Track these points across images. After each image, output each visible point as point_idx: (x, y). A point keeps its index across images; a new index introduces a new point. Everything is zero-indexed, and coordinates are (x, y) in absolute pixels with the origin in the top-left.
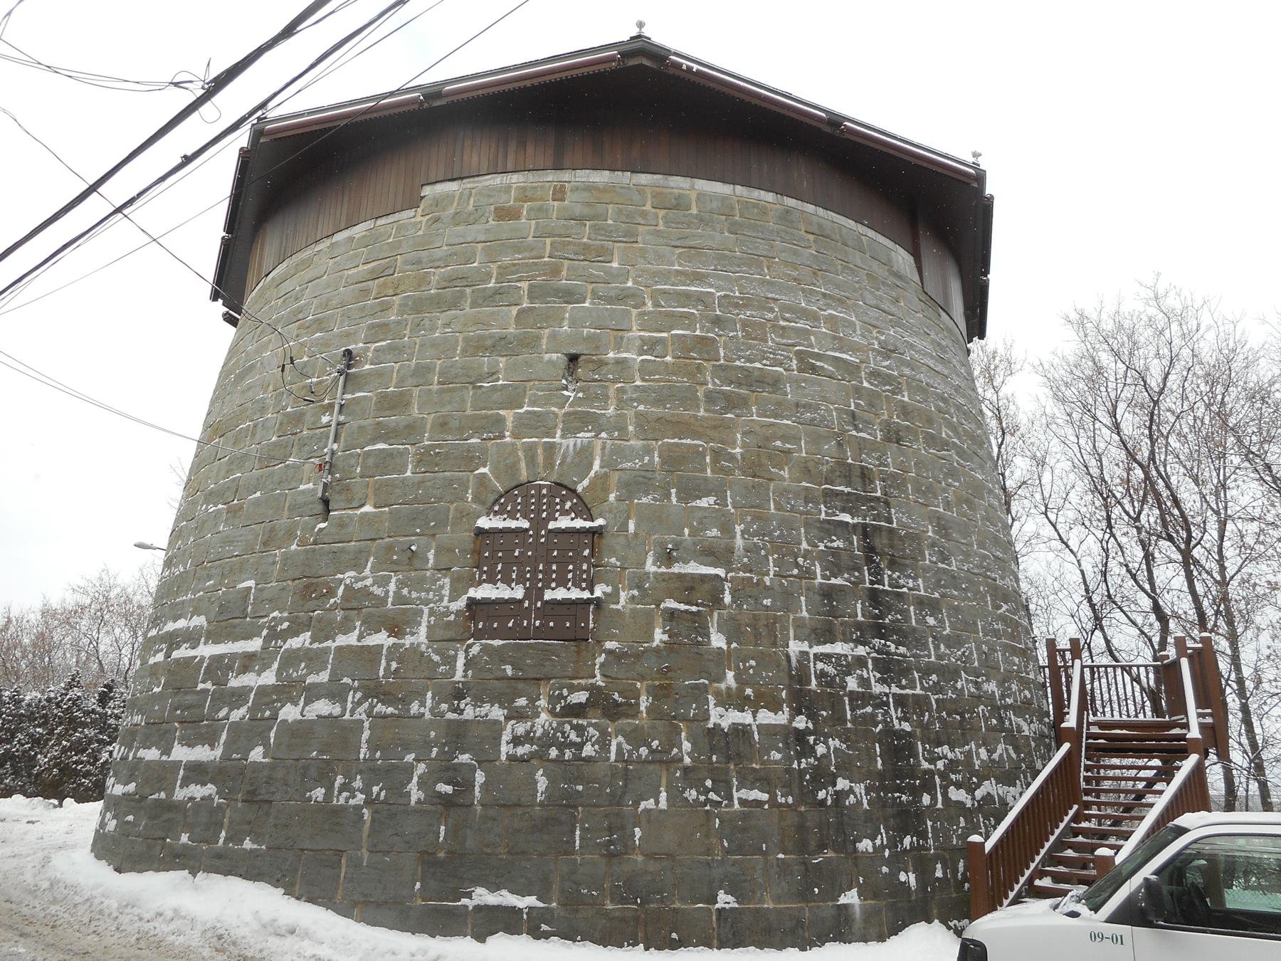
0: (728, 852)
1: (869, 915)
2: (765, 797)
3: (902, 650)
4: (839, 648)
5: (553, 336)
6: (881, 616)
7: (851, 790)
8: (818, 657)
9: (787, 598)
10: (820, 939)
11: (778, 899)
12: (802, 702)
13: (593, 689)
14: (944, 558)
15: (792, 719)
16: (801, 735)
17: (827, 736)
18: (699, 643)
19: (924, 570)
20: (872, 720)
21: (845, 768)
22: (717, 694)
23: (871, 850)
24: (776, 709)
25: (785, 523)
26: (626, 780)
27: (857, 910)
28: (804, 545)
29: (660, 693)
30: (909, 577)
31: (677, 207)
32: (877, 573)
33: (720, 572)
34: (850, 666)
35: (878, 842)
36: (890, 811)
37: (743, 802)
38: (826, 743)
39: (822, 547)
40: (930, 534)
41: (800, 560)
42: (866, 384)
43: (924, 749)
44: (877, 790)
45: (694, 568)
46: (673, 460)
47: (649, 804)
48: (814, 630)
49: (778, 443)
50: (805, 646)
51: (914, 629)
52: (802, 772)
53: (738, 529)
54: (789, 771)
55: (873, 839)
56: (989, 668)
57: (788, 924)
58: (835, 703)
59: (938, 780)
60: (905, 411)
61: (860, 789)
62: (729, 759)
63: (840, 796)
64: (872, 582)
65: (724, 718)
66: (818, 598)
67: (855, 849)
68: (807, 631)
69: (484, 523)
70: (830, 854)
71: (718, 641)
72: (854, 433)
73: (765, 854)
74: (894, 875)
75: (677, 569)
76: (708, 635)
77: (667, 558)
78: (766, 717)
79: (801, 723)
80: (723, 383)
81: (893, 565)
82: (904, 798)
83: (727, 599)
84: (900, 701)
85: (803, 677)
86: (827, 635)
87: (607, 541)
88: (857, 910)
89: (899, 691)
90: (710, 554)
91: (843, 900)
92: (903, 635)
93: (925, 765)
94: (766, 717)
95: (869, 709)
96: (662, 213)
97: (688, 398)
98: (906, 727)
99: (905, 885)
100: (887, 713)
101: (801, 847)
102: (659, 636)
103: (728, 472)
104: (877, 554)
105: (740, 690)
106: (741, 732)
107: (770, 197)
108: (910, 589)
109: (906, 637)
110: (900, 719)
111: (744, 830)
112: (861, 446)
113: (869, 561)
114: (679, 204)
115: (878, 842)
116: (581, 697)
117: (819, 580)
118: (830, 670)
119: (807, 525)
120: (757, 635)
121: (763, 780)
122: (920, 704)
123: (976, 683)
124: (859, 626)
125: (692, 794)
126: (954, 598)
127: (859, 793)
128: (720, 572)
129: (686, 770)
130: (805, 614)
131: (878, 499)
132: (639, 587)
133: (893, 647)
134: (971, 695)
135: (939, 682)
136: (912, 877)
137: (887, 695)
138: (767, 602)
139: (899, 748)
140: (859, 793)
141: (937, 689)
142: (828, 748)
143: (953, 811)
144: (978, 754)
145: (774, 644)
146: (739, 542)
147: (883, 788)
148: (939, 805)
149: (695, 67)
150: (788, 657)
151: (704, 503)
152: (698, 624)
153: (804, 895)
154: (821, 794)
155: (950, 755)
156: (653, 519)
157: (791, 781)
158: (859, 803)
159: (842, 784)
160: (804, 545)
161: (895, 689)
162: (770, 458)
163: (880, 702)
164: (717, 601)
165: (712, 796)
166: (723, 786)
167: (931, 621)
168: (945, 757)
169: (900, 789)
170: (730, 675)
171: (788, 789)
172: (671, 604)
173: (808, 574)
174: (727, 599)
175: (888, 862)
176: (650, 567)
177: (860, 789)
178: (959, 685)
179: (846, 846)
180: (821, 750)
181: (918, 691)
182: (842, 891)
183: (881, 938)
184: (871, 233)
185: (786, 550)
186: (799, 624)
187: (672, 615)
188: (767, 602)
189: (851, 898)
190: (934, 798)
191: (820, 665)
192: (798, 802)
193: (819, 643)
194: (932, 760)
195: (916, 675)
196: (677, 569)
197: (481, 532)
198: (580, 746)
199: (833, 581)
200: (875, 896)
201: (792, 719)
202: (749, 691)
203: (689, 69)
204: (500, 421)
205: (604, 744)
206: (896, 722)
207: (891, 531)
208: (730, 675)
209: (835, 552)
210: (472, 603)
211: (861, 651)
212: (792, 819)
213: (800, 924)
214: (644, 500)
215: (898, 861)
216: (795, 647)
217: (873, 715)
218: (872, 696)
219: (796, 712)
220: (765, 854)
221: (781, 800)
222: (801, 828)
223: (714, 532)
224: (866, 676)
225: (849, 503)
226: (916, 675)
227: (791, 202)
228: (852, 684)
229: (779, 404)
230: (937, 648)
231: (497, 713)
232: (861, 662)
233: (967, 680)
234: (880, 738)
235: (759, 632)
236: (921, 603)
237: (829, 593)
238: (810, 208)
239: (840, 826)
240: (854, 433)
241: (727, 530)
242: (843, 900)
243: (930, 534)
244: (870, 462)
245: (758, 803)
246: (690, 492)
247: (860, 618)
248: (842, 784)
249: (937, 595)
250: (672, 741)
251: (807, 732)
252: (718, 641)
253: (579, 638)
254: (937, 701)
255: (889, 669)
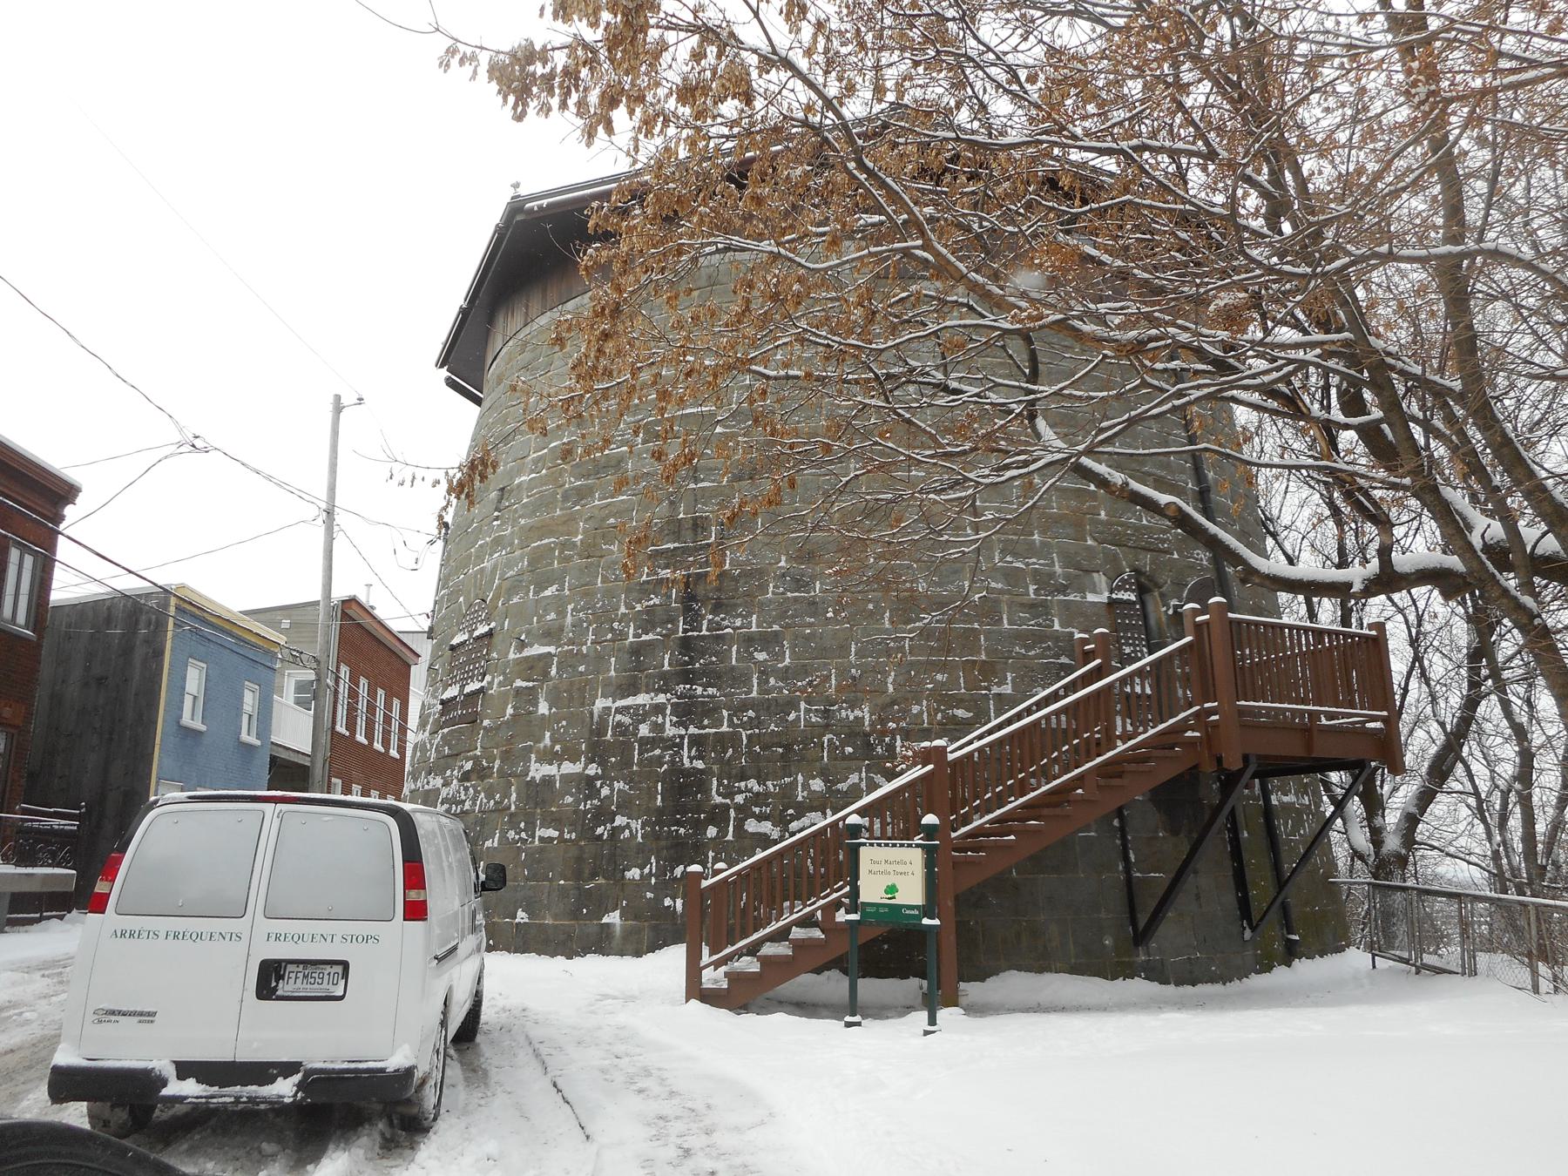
0: (527, 879)
1: (628, 934)
2: (556, 834)
3: (711, 691)
4: (642, 699)
6: (692, 661)
7: (628, 826)
8: (618, 711)
9: (599, 661)
10: (584, 951)
11: (555, 917)
12: (597, 752)
13: (476, 759)
14: (800, 583)
15: (585, 768)
16: (590, 780)
17: (612, 780)
18: (531, 713)
19: (761, 604)
20: (659, 761)
21: (625, 806)
22: (538, 752)
23: (637, 877)
24: (574, 761)
25: (610, 594)
26: (482, 826)
27: (618, 929)
28: (623, 610)
29: (506, 756)
30: (740, 615)
32: (694, 621)
33: (552, 649)
34: (640, 715)
35: (646, 870)
36: (663, 843)
37: (542, 839)
38: (611, 787)
39: (638, 607)
40: (783, 564)
41: (616, 625)
43: (720, 784)
44: (653, 825)
45: (538, 650)
46: (537, 559)
47: (488, 844)
48: (619, 686)
49: (612, 520)
50: (608, 702)
51: (733, 668)
52: (586, 812)
53: (570, 607)
54: (576, 812)
55: (642, 869)
56: (853, 692)
57: (562, 937)
58: (625, 749)
59: (732, 813)
61: (636, 825)
62: (536, 805)
63: (616, 832)
64: (685, 631)
65: (538, 771)
66: (627, 656)
67: (623, 877)
68: (612, 689)
69: (455, 642)
70: (601, 881)
71: (543, 708)
72: (692, 486)
73: (550, 880)
74: (658, 900)
75: (528, 652)
76: (536, 705)
77: (522, 645)
78: (569, 768)
79: (593, 770)
80: (578, 479)
81: (715, 611)
82: (682, 831)
83: (553, 672)
84: (696, 741)
85: (601, 731)
86: (631, 688)
87: (497, 639)
88: (618, 929)
89: (697, 731)
90: (551, 634)
91: (605, 920)
92: (713, 677)
93: (718, 800)
94: (569, 768)
95: (657, 752)
98: (700, 764)
99: (670, 911)
100: (677, 753)
101: (578, 876)
102: (510, 711)
103: (568, 559)
104: (697, 602)
105: (553, 747)
106: (548, 781)
108: (734, 629)
109: (719, 677)
110: (691, 759)
111: (539, 862)
112: (698, 496)
113: (687, 609)
115: (646, 870)
116: (468, 766)
117: (631, 639)
118: (627, 720)
119: (628, 591)
120: (571, 699)
121: (555, 821)
122: (722, 741)
123: (827, 711)
124: (663, 676)
125: (511, 834)
126: (810, 625)
127: (633, 827)
128: (552, 649)
129: (512, 815)
130: (613, 673)
131: (709, 545)
132: (504, 673)
133: (699, 690)
134: (813, 725)
135: (758, 717)
136: (679, 902)
137: (682, 737)
138: (582, 668)
139: (685, 786)
140: (633, 827)
141: (751, 724)
142: (612, 790)
143: (747, 842)
144: (806, 786)
145: (583, 705)
146: (569, 619)
147: (659, 822)
148: (730, 837)
149: (545, 202)
150: (592, 714)
151: (548, 593)
152: (529, 696)
153: (575, 914)
154: (600, 830)
155: (756, 788)
156: (520, 614)
157: (577, 820)
158: (633, 836)
159: (620, 820)
160: (623, 610)
161: (692, 730)
162: (603, 537)
163: (674, 745)
164: (546, 674)
165: (523, 835)
166: (531, 830)
167: (761, 656)
168: (750, 791)
169: (679, 824)
170: (548, 734)
171: (573, 826)
172: (519, 683)
173: (622, 635)
174: (553, 672)
175: (654, 889)
176: (512, 656)
177: (636, 825)
178: (792, 716)
179: (616, 874)
180: (605, 791)
181: (725, 728)
182: (607, 911)
183: (638, 954)
185: (604, 618)
186: (607, 683)
187: (518, 691)
188: (582, 668)
189: (613, 918)
190: (723, 832)
191: (619, 717)
192: (579, 838)
193: (623, 697)
194: (730, 794)
195: (725, 713)
196: (528, 652)
197: (453, 648)
198: (463, 802)
199: (644, 637)
200: (636, 918)
201: (585, 768)
202: (558, 747)
203: (540, 207)
205: (474, 800)
206: (686, 761)
207: (722, 575)
208: (548, 734)
209: (650, 611)
210: (443, 702)
211: (661, 698)
212: (573, 852)
213: (570, 938)
214: (515, 600)
215: (667, 886)
216: (600, 703)
217: (661, 757)
218: (662, 739)
219: (591, 761)
220: (550, 880)
221: (567, 836)
222: (580, 859)
223: (553, 616)
224: (660, 720)
225: (671, 559)
226: (725, 713)
228: (644, 730)
230: (763, 682)
231: (439, 781)
232: (659, 709)
233: (807, 711)
234: (663, 778)
235: (573, 696)
236: (749, 641)
237: (638, 650)
239: (614, 856)
240: (692, 486)
241: (561, 614)
242: (605, 920)
243: (783, 564)
244: (706, 510)
245: (551, 839)
246: (541, 587)
247: (667, 667)
248: (620, 820)
249: (776, 627)
250: (507, 795)
251: (597, 777)
252: (543, 708)
253: (473, 720)
254: (749, 737)
255: (687, 711)
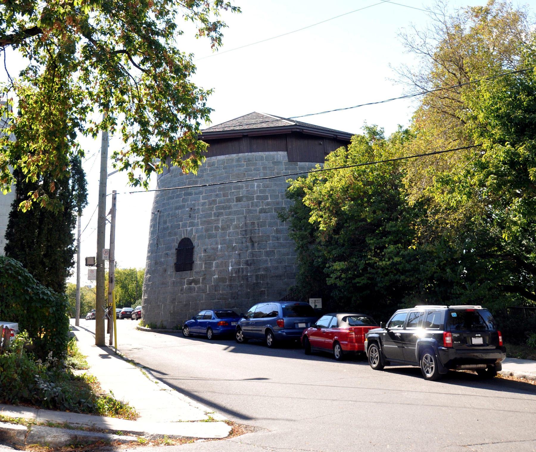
5: (188, 204)
31: (213, 165)
42: (255, 200)
60: (268, 204)
96: (209, 168)
97: (210, 216)
107: (234, 156)
114: (213, 164)
184: (267, 153)
204: (179, 224)
227: (241, 155)
229: (230, 212)
238: (247, 154)
